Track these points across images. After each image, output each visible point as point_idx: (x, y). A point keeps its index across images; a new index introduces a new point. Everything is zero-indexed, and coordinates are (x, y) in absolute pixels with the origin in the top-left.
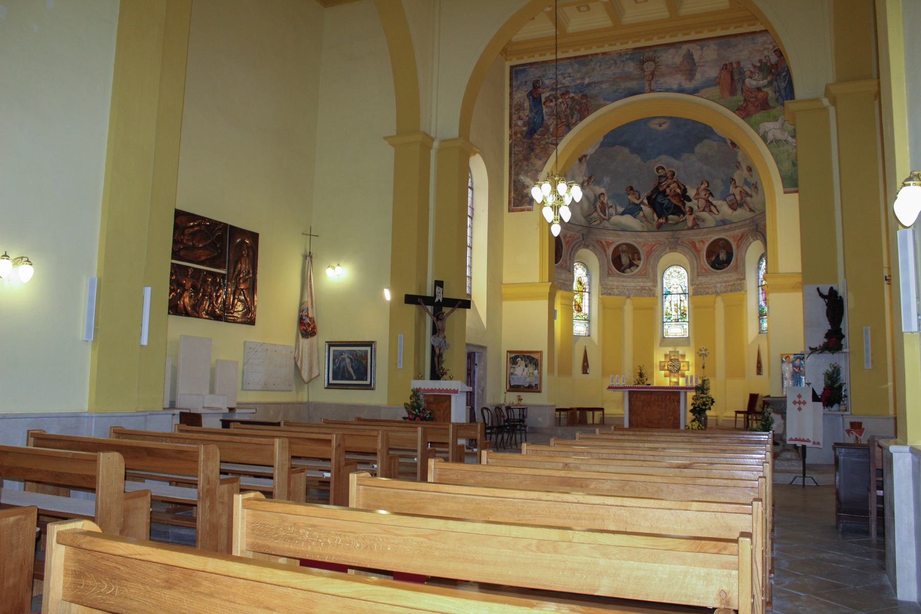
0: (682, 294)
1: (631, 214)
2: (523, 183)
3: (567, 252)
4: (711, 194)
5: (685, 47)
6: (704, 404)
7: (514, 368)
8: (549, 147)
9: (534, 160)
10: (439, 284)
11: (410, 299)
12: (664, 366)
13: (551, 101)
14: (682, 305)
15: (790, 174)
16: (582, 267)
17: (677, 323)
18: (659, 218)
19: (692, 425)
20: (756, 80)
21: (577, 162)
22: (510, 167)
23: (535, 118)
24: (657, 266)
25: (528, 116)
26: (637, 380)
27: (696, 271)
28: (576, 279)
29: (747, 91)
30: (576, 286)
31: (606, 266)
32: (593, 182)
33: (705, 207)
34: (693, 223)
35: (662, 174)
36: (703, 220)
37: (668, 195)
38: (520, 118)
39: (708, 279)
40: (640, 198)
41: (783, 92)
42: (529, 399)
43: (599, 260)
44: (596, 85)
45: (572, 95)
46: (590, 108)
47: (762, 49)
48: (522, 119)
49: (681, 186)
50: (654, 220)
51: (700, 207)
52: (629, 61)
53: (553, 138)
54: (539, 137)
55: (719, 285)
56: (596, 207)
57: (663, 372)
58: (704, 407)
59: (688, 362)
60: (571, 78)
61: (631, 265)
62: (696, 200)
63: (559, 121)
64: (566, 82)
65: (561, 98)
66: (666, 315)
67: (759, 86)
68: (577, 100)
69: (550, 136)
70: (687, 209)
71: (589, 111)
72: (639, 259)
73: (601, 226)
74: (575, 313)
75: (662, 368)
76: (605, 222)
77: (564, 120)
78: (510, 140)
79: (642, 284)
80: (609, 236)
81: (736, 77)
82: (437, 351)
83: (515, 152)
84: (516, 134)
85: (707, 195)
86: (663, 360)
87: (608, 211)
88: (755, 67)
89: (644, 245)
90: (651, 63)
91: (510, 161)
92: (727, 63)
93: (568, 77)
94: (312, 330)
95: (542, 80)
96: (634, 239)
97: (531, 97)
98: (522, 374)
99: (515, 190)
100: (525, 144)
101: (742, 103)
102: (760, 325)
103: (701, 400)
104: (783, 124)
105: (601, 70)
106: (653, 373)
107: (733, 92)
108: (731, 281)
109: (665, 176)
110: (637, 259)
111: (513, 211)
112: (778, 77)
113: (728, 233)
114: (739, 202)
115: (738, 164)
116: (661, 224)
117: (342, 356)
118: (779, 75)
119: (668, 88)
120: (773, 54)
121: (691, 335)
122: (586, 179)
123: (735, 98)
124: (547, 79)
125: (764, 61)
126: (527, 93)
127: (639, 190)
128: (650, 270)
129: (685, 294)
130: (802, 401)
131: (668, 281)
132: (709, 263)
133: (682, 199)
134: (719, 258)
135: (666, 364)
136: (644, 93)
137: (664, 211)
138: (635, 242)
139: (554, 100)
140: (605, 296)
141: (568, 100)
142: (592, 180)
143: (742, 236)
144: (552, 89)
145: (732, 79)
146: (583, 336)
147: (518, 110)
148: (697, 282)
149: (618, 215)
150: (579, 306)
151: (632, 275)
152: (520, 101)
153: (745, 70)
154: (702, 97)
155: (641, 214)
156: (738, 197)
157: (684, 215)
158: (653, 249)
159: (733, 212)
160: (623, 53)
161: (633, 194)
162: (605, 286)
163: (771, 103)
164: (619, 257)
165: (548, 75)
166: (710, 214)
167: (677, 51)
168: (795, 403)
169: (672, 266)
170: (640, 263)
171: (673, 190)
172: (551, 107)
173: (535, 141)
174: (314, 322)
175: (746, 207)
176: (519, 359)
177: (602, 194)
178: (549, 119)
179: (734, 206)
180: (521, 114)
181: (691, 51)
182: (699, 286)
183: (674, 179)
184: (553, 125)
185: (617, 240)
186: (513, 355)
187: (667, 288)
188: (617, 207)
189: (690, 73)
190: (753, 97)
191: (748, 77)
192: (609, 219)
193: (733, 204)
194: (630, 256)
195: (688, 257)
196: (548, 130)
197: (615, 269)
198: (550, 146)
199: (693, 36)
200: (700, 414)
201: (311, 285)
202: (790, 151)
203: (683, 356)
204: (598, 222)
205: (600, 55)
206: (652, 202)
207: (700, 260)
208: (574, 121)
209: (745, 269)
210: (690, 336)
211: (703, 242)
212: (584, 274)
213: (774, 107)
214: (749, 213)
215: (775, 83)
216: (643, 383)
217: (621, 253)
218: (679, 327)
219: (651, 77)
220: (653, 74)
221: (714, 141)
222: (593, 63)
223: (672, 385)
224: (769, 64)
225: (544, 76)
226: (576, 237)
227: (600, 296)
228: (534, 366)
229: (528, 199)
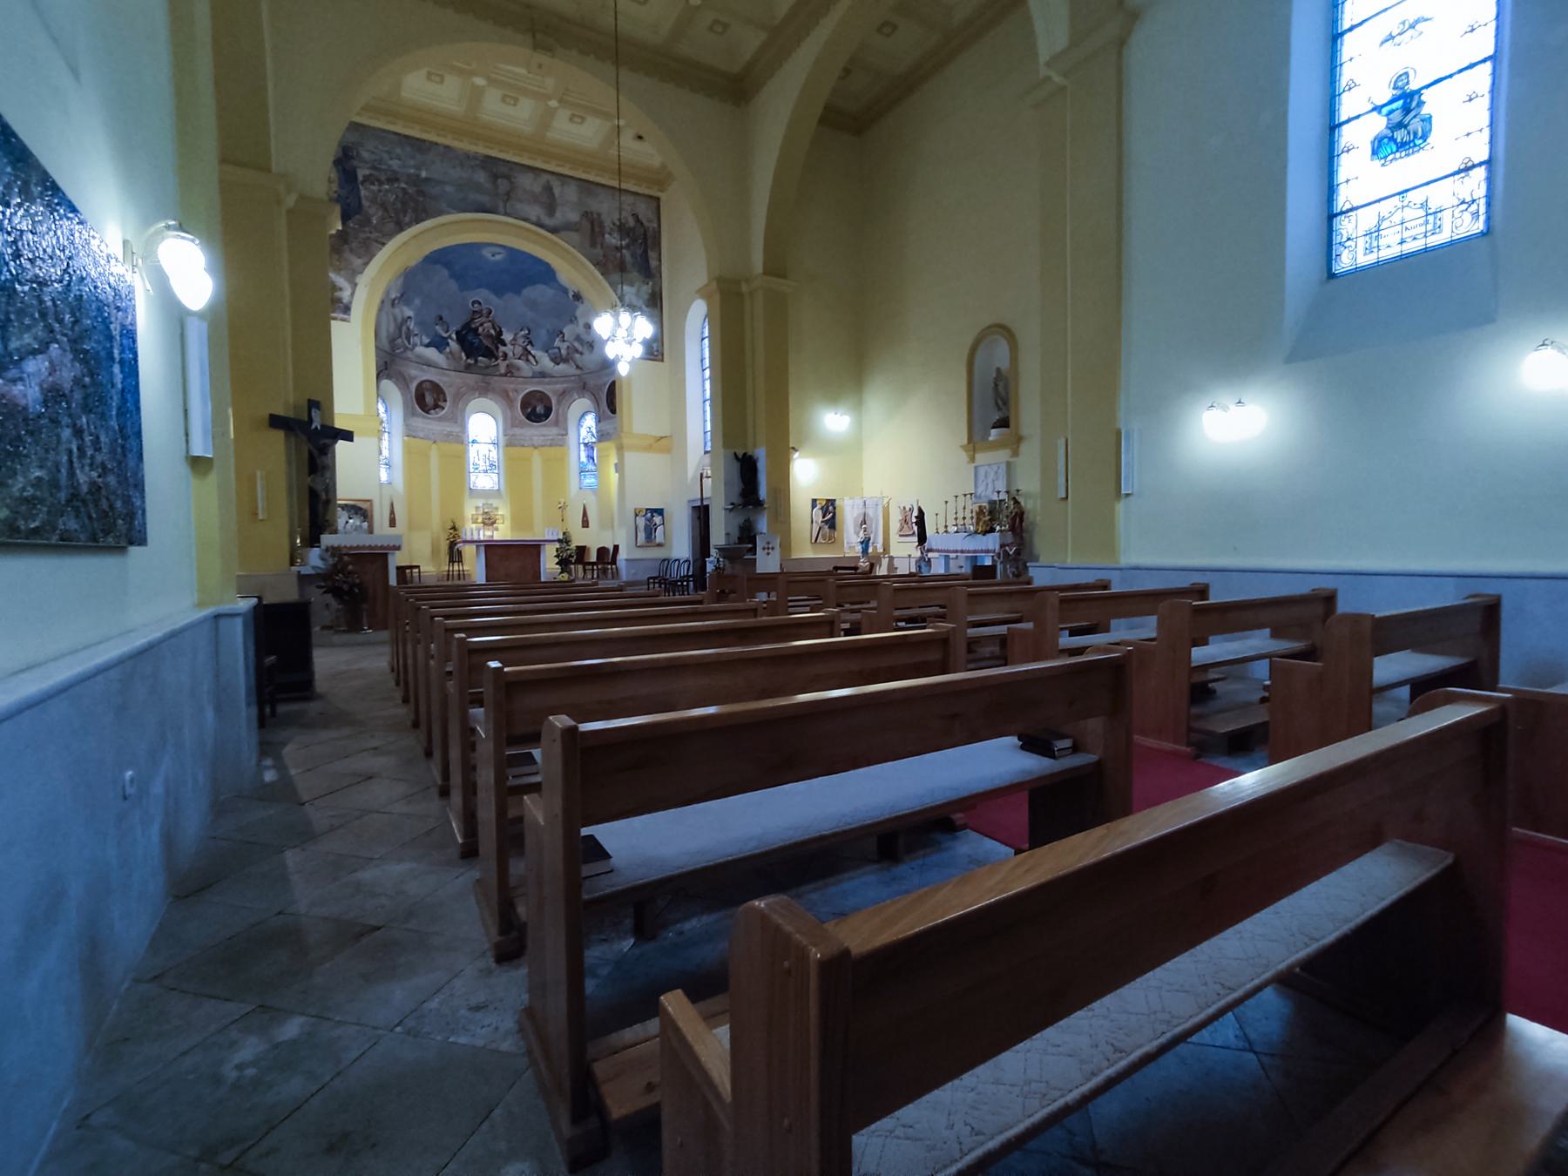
1: (437, 348)
4: (530, 343)
5: (545, 177)
9: (347, 255)
10: (313, 404)
11: (276, 422)
12: (477, 519)
13: (374, 185)
18: (468, 358)
20: (614, 238)
25: (335, 192)
36: (518, 369)
37: (479, 335)
39: (522, 431)
41: (639, 258)
43: (402, 394)
45: (403, 185)
50: (461, 359)
53: (377, 234)
54: (356, 226)
55: (535, 438)
59: (502, 515)
61: (436, 406)
62: (512, 345)
64: (395, 164)
65: (388, 184)
69: (373, 230)
70: (501, 354)
72: (445, 401)
75: (475, 522)
79: (449, 429)
81: (597, 229)
82: (323, 496)
86: (474, 513)
88: (614, 224)
90: (505, 181)
92: (589, 210)
96: (438, 377)
104: (638, 291)
107: (593, 244)
113: (548, 387)
114: (564, 357)
116: (470, 365)
118: (636, 240)
121: (502, 488)
122: (399, 295)
125: (623, 221)
130: (770, 546)
139: (376, 183)
143: (564, 392)
144: (374, 168)
145: (593, 230)
148: (511, 433)
151: (439, 418)
155: (448, 350)
156: (564, 352)
157: (496, 360)
163: (629, 266)
172: (373, 191)
175: (573, 364)
177: (409, 318)
178: (369, 207)
179: (557, 360)
183: (490, 319)
185: (419, 375)
188: (424, 337)
189: (551, 208)
192: (413, 348)
196: (369, 221)
197: (420, 411)
200: (566, 565)
203: (497, 509)
204: (402, 349)
206: (461, 339)
208: (407, 219)
210: (502, 488)
211: (516, 391)
215: (632, 247)
220: (508, 194)
223: (486, 539)
229: (341, 305)
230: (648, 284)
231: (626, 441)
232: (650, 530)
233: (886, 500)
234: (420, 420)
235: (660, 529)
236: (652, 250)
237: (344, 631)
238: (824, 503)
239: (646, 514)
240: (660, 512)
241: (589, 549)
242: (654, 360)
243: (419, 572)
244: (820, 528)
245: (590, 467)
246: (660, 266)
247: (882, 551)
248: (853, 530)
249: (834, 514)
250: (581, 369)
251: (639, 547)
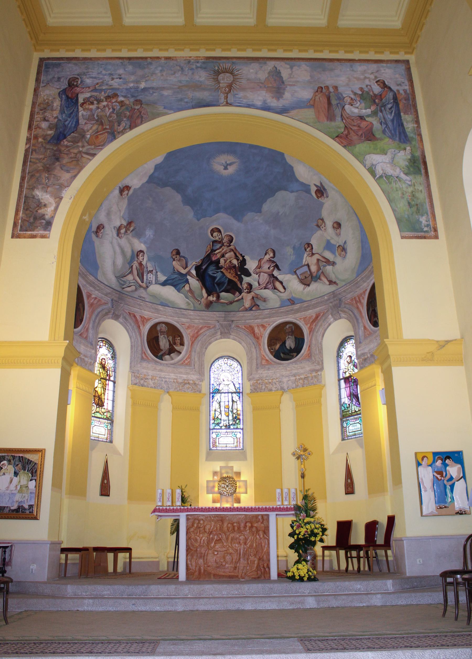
0: (235, 393)
1: (175, 286)
2: (39, 200)
3: (90, 318)
4: (277, 267)
5: (271, 64)
8: (82, 156)
9: (58, 171)
12: (214, 487)
13: (92, 103)
14: (235, 406)
15: (406, 216)
16: (107, 346)
17: (228, 431)
18: (209, 295)
20: (358, 108)
21: (117, 192)
22: (23, 179)
23: (67, 120)
24: (204, 354)
25: (57, 117)
27: (255, 361)
28: (98, 361)
29: (348, 118)
30: (97, 368)
31: (140, 348)
32: (132, 231)
33: (267, 283)
34: (252, 304)
35: (217, 238)
36: (265, 300)
37: (221, 268)
38: (45, 120)
39: (270, 372)
40: (186, 267)
41: (390, 124)
43: (130, 338)
44: (154, 91)
45: (121, 99)
46: (144, 116)
47: (362, 77)
48: (48, 121)
49: (240, 257)
51: (261, 284)
52: (199, 69)
53: (89, 147)
54: (69, 144)
55: (285, 380)
56: (132, 266)
57: (210, 496)
59: (245, 482)
60: (121, 80)
61: (171, 351)
62: (257, 274)
63: (100, 127)
64: (115, 83)
65: (106, 101)
66: (214, 419)
67: (362, 115)
68: (127, 105)
69: (86, 144)
70: (245, 286)
71: (143, 120)
72: (182, 344)
73: (136, 295)
74: (94, 408)
75: (210, 490)
76: (142, 290)
77: (108, 127)
78: (26, 144)
79: (185, 376)
80: (145, 311)
81: (334, 102)
83: (32, 160)
84: (36, 137)
85: (273, 268)
86: (211, 479)
87: (147, 275)
88: (355, 94)
89: (189, 328)
90: (228, 75)
91: (23, 171)
93: (117, 78)
95: (81, 78)
97: (64, 96)
99: (26, 209)
100: (49, 150)
101: (343, 130)
104: (393, 159)
105: (162, 75)
106: (198, 496)
107: (331, 117)
108: (301, 374)
109: (220, 242)
110: (179, 343)
111: (18, 237)
112: (383, 108)
113: (298, 315)
114: (314, 275)
115: (320, 221)
116: (211, 302)
118: (384, 106)
119: (251, 103)
120: (376, 84)
122: (125, 223)
123: (333, 124)
124: (88, 78)
125: (366, 89)
126: (59, 90)
127: (187, 256)
128: (196, 359)
129: (239, 393)
131: (216, 376)
132: (271, 353)
133: (239, 273)
134: (286, 347)
135: (217, 485)
136: (219, 106)
137: (215, 285)
138: (178, 322)
139: (95, 102)
140: (136, 387)
141: (114, 104)
142: (132, 229)
144: (95, 90)
145: (329, 103)
146: (102, 441)
147: (44, 110)
148: (257, 376)
149: (157, 284)
150: (100, 398)
152: (47, 99)
153: (344, 96)
154: (293, 118)
155: (187, 287)
156: (314, 268)
157: (240, 293)
158: (199, 333)
159: (304, 289)
160: (192, 61)
161: (179, 260)
162: (136, 374)
163: (378, 134)
164: (157, 339)
165: (90, 73)
166: (274, 293)
167: (262, 67)
169: (221, 357)
170: (183, 350)
171: (228, 261)
172: (91, 110)
173: (63, 149)
175: (323, 278)
177: (141, 251)
178: (86, 123)
180: (48, 114)
181: (278, 69)
182: (259, 382)
183: (232, 247)
184: (91, 131)
187: (215, 385)
188: (159, 273)
190: (354, 126)
191: (347, 103)
192: (147, 287)
193: (306, 277)
194: (171, 338)
195: (245, 345)
196: (83, 136)
198: (85, 156)
199: (280, 54)
202: (404, 189)
203: (238, 474)
204: (133, 288)
205: (163, 59)
207: (260, 349)
208: (121, 128)
209: (322, 357)
211: (263, 326)
212: (109, 356)
213: (381, 139)
214: (328, 286)
217: (159, 334)
218: (231, 435)
219: (227, 89)
220: (230, 86)
221: (292, 192)
222: (152, 67)
224: (371, 93)
225: (84, 74)
226: (103, 301)
227: (131, 385)
229: (44, 221)
230: (405, 149)
231: (392, 350)
234: (150, 365)
236: (405, 113)
242: (425, 238)
245: (354, 408)
246: (419, 127)
250: (335, 283)
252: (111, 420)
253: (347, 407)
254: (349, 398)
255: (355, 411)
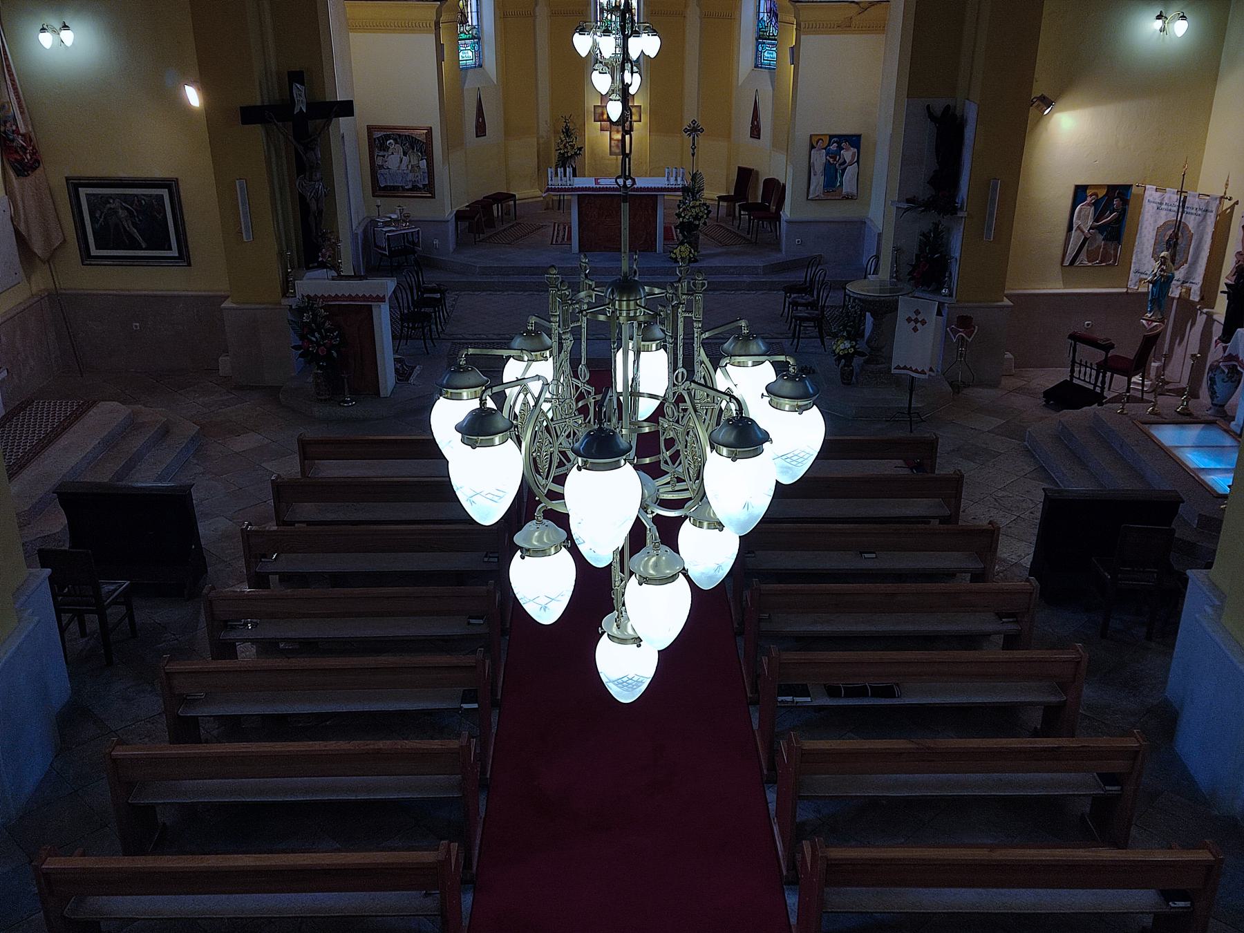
6: (697, 217)
7: (384, 156)
10: (297, 77)
11: (250, 115)
19: (680, 251)
26: (562, 141)
42: (419, 209)
58: (697, 222)
82: (313, 206)
94: (31, 158)
98: (399, 167)
102: (758, 55)
103: (693, 210)
117: (108, 205)
168: (909, 320)
174: (31, 141)
176: (391, 141)
186: (378, 134)
201: (8, 66)
216: (572, 147)
228: (419, 154)
232: (832, 174)
233: (1227, 204)
235: (851, 171)
237: (325, 400)
238: (1102, 193)
239: (829, 145)
240: (854, 140)
241: (757, 173)
243: (515, 203)
244: (1085, 239)
247: (1197, 299)
248: (1151, 250)
249: (1123, 213)
251: (812, 200)
252: (477, 38)
253: (766, 27)
254: (769, 14)
255: (773, 35)
